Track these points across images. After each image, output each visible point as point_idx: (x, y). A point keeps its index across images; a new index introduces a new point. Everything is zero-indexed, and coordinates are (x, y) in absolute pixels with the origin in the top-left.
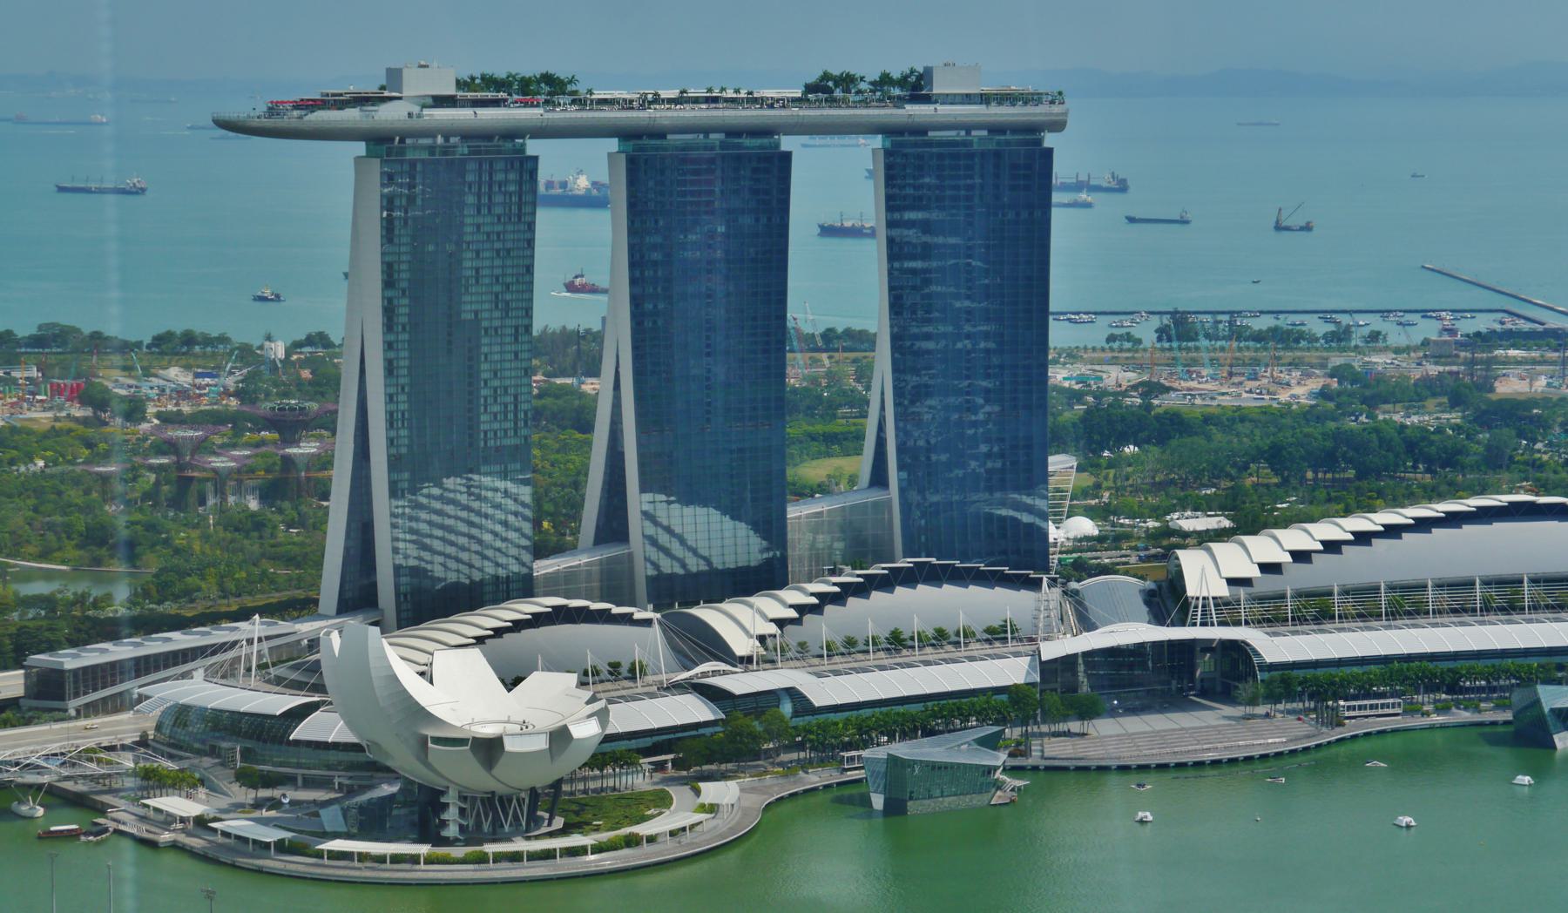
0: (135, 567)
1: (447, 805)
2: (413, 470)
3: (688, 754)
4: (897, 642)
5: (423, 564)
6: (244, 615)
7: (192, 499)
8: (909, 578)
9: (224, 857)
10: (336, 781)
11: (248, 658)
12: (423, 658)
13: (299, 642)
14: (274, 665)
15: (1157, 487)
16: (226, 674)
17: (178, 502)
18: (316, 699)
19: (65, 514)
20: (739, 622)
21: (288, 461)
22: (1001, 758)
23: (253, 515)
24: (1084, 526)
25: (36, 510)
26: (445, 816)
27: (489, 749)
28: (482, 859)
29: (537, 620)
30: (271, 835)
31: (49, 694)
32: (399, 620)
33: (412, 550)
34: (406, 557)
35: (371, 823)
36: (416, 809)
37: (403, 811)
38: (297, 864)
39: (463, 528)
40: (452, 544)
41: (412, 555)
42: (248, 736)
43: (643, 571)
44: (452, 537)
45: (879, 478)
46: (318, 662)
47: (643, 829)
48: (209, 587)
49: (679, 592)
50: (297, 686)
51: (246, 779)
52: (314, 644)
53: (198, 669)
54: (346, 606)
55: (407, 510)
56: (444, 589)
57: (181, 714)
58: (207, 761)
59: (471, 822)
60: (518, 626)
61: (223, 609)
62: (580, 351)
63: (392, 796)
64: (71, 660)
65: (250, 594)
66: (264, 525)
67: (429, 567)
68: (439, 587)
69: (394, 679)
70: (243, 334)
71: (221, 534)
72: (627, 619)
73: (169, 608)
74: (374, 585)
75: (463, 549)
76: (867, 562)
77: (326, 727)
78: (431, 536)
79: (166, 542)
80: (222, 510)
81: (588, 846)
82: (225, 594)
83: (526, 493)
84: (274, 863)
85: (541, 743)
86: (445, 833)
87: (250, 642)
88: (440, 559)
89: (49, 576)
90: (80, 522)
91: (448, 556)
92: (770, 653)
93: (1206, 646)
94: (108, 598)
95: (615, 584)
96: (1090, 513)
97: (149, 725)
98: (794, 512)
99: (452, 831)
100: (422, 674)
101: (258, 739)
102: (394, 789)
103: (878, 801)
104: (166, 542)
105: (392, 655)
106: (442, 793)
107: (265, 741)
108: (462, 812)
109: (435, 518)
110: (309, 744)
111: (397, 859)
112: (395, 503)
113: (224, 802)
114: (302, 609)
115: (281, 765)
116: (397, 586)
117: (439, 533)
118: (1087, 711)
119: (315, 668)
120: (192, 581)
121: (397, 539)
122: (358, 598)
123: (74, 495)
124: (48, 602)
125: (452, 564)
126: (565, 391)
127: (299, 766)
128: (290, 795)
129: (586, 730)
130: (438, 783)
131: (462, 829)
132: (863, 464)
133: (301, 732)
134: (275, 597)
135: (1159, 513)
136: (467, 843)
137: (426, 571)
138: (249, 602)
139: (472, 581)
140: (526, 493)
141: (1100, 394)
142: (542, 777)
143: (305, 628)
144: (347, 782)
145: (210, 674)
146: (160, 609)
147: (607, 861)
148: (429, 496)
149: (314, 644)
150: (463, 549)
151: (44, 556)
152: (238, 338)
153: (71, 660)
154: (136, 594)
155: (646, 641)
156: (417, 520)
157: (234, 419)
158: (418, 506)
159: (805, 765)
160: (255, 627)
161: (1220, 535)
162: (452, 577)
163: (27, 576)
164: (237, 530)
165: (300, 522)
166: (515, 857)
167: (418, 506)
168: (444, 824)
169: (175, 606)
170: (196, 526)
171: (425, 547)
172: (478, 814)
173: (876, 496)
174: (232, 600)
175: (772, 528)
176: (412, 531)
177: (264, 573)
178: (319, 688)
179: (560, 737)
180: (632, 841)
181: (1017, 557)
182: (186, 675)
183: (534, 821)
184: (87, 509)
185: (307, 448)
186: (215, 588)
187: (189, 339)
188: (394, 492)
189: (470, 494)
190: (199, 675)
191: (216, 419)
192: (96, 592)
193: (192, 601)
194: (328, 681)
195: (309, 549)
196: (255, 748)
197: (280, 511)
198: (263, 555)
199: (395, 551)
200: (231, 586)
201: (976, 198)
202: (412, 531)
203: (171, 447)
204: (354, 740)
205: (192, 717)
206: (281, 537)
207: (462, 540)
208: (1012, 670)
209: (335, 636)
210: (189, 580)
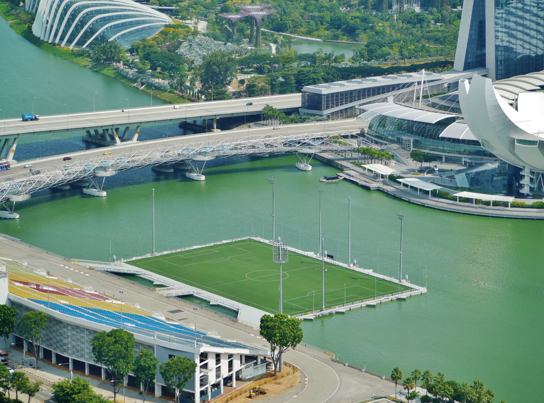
0: (355, 40)
1: (524, 176)
5: (511, 46)
7: (385, 5)
9: (398, 194)
10: (463, 160)
11: (418, 93)
12: (512, 96)
13: (444, 84)
14: (431, 96)
16: (407, 100)
18: (454, 116)
19: (320, 12)
23: (418, 15)
25: (305, 9)
26: (522, 182)
30: (430, 187)
32: (497, 75)
33: (505, 38)
34: (502, 41)
36: (506, 177)
37: (500, 178)
39: (534, 26)
40: (527, 35)
41: (505, 40)
42: (417, 134)
44: (528, 31)
46: (457, 96)
48: (394, 52)
51: (415, 156)
53: (390, 96)
54: (468, 66)
55: (504, 15)
56: (522, 58)
57: (383, 120)
58: (395, 146)
59: (535, 186)
61: (402, 65)
63: (493, 170)
65: (416, 57)
66: (423, 21)
67: (514, 47)
68: (519, 57)
69: (498, 107)
71: (401, 25)
73: (374, 63)
74: (484, 55)
75: (533, 37)
77: (459, 130)
78: (516, 30)
79: (372, 28)
82: (403, 57)
84: (431, 201)
86: (522, 191)
87: (419, 83)
88: (521, 43)
89: (310, 43)
90: (328, 16)
91: (525, 41)
94: (343, 56)
97: (365, 126)
99: (525, 190)
100: (511, 105)
101: (423, 136)
102: (495, 165)
104: (372, 28)
105: (497, 93)
106: (521, 170)
107: (426, 137)
108: (532, 180)
109: (519, 20)
110: (449, 139)
111: (496, 204)
112: (498, 11)
113: (404, 168)
114: (443, 67)
115: (434, 150)
116: (497, 57)
117: (520, 28)
119: (455, 99)
120: (386, 49)
121: (498, 31)
122: (475, 62)
124: (312, 58)
125: (527, 46)
127: (444, 151)
130: (519, 164)
131: (531, 189)
133: (446, 133)
134: (429, 60)
136: (534, 197)
137: (512, 49)
138: (415, 62)
139: (537, 56)
143: (447, 77)
144: (468, 161)
145: (397, 100)
146: (369, 63)
148: (516, 8)
150: (533, 37)
151: (309, 33)
154: (356, 56)
156: (509, 21)
158: (509, 13)
160: (422, 75)
162: (527, 52)
163: (300, 42)
164: (409, 22)
165: (442, 20)
167: (509, 13)
168: (521, 186)
169: (377, 62)
170: (387, 20)
171: (512, 36)
172: (540, 182)
174: (406, 60)
176: (506, 27)
177: (423, 46)
178: (457, 110)
182: (385, 100)
184: (331, 9)
186: (398, 54)
189: (538, 8)
190: (391, 99)
192: (337, 54)
193: (385, 60)
194: (462, 106)
195: (447, 34)
197: (431, 13)
198: (422, 37)
199: (497, 37)
200: (406, 53)
202: (506, 27)
204: (473, 138)
205: (388, 122)
206: (432, 27)
207: (533, 33)
209: (467, 82)
210: (384, 48)
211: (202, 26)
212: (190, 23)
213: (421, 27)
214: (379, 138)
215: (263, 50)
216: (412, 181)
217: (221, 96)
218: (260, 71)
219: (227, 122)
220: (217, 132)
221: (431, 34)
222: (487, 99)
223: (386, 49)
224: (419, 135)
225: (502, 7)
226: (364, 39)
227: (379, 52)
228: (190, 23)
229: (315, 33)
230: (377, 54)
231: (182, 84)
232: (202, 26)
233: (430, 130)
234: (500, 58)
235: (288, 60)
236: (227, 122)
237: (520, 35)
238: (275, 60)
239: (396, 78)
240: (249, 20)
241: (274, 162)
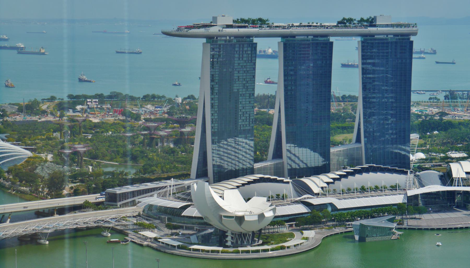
0: (137, 164)
1: (227, 236)
2: (218, 136)
3: (300, 222)
4: (363, 190)
5: (221, 164)
6: (169, 178)
7: (154, 143)
8: (367, 170)
10: (195, 228)
11: (170, 191)
12: (221, 192)
14: (177, 193)
15: (444, 144)
16: (164, 196)
17: (150, 145)
18: (189, 203)
19: (117, 148)
20: (315, 183)
21: (182, 133)
22: (394, 225)
23: (172, 149)
24: (421, 155)
25: (109, 146)
26: (227, 239)
27: (240, 219)
28: (238, 252)
29: (255, 181)
30: (176, 244)
31: (113, 200)
33: (218, 160)
34: (216, 162)
35: (205, 240)
37: (215, 237)
38: (184, 252)
39: (233, 153)
40: (230, 158)
41: (218, 162)
42: (169, 214)
43: (287, 167)
44: (230, 156)
45: (358, 140)
46: (190, 193)
47: (286, 244)
48: (158, 170)
49: (298, 173)
50: (184, 200)
51: (169, 227)
52: (189, 187)
53: (155, 194)
54: (199, 176)
56: (227, 171)
57: (150, 207)
58: (157, 221)
59: (235, 241)
60: (249, 183)
61: (163, 177)
62: (269, 101)
63: (211, 233)
64: (118, 191)
65: (170, 172)
67: (223, 165)
68: (226, 171)
70: (169, 95)
71: (162, 154)
72: (282, 182)
73: (147, 176)
74: (207, 170)
75: (233, 160)
76: (355, 165)
77: (192, 212)
78: (224, 156)
79: (146, 156)
80: (162, 147)
81: (269, 249)
82: (163, 172)
83: (252, 143)
84: (177, 252)
85: (256, 218)
86: (227, 244)
87: (170, 186)
88: (226, 163)
89: (112, 166)
91: (229, 162)
92: (324, 192)
93: (459, 192)
95: (278, 171)
96: (423, 151)
98: (333, 150)
99: (229, 244)
100: (221, 197)
101: (173, 215)
103: (357, 238)
104: (146, 156)
105: (212, 191)
106: (226, 232)
107: (174, 216)
108: (232, 238)
109: (225, 150)
111: (213, 251)
113: (162, 233)
116: (214, 170)
117: (226, 155)
118: (420, 212)
119: (189, 194)
120: (154, 168)
121: (214, 157)
122: (202, 174)
123: (120, 142)
124: (112, 173)
125: (230, 164)
126: (264, 113)
127: (184, 223)
128: (181, 232)
129: (269, 215)
130: (225, 229)
131: (232, 243)
132: (353, 136)
133: (185, 213)
134: (178, 173)
135: (444, 152)
136: (234, 247)
137: (222, 166)
138: (170, 174)
139: (236, 170)
140: (252, 143)
141: (426, 116)
142: (256, 228)
143: (186, 182)
144: (198, 228)
145: (159, 195)
146: (144, 176)
147: (275, 253)
148: (223, 144)
149: (189, 187)
150: (233, 160)
151: (111, 160)
152: (168, 96)
153: (118, 191)
154: (137, 172)
155: (288, 188)
156: (220, 151)
157: (167, 121)
158: (220, 147)
159: (335, 226)
160: (172, 182)
161: (463, 159)
162: (230, 168)
163: (106, 166)
164: (167, 153)
165: (185, 151)
166: (248, 252)
167: (220, 147)
168: (227, 241)
169: (149, 175)
170: (155, 152)
171: (222, 159)
172: (237, 239)
173: (358, 145)
174: (165, 174)
175: (326, 155)
176: (218, 154)
177: (175, 166)
178: (190, 200)
179: (261, 216)
180: (282, 248)
181: (401, 165)
182: (152, 196)
183: (253, 241)
185: (187, 129)
186: (160, 170)
187: (154, 97)
188: (213, 142)
189: (235, 143)
191: (162, 120)
192: (126, 171)
193: (154, 174)
194: (193, 198)
195: (188, 159)
196: (171, 218)
197: (179, 148)
198: (174, 161)
199: (213, 160)
200: (165, 170)
201: (389, 56)
202: (218, 154)
203: (148, 128)
205: (153, 208)
206: (180, 155)
207: (233, 157)
208: (398, 199)
209: (195, 186)
210: (153, 168)
211: (50, 157)
212: (43, 156)
213: (174, 155)
214: (148, 217)
215: (85, 170)
216: (166, 240)
217: (60, 196)
218: (82, 181)
219: (61, 211)
220: (56, 216)
221: (179, 159)
222: (206, 193)
223: (154, 168)
224: (170, 215)
225: (216, 144)
226: (142, 163)
227: (150, 170)
228: (43, 156)
229: (115, 160)
230: (149, 171)
231: (37, 189)
232: (50, 157)
233: (176, 212)
234: (215, 171)
235: (99, 175)
236: (61, 211)
237: (226, 158)
238: (91, 175)
239: (158, 184)
240: (76, 153)
241: (89, 232)
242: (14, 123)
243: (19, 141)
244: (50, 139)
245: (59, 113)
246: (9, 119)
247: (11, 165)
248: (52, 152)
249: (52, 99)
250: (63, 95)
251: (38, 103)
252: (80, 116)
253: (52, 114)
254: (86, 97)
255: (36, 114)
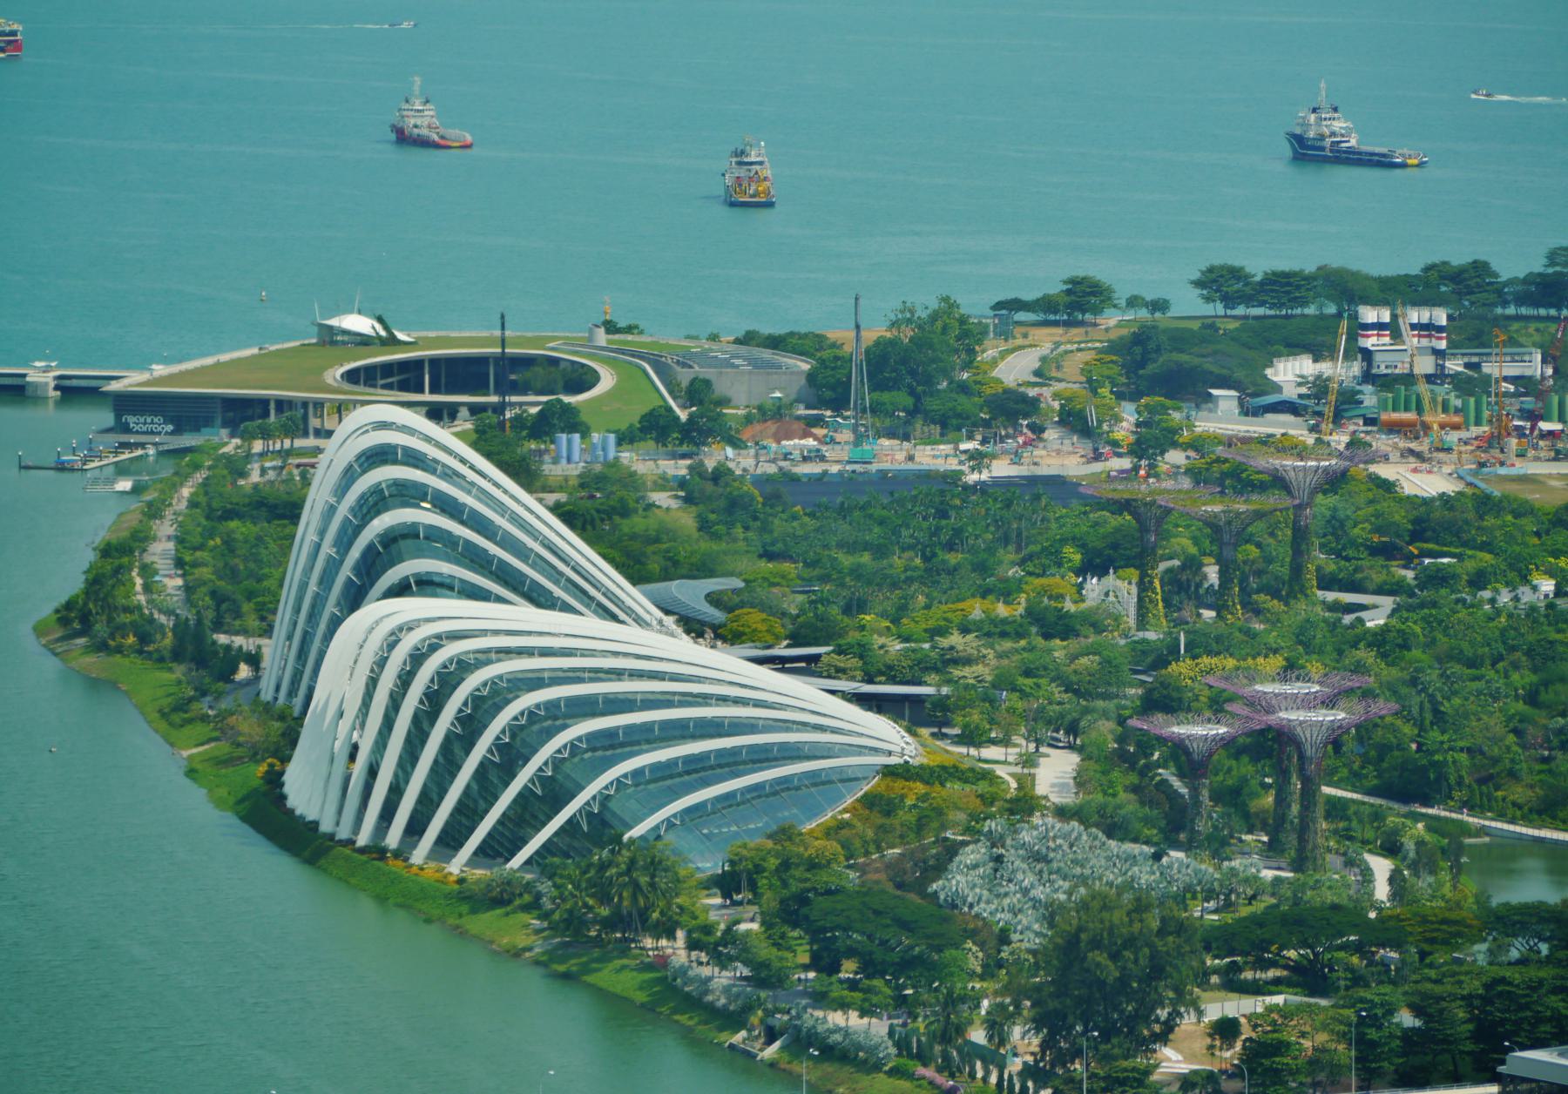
25: (1532, 698)
211: (1056, 772)
215: (1331, 880)
218: (1310, 978)
231: (950, 1032)
232: (1056, 772)
235: (1445, 931)
238: (1388, 931)
240: (1271, 745)
242: (780, 489)
243: (807, 644)
244: (1057, 626)
245: (1129, 415)
246: (742, 462)
247: (752, 833)
248: (1071, 730)
249: (1079, 300)
250: (1160, 277)
251: (969, 336)
252: (1302, 449)
253: (1074, 421)
254: (1348, 289)
255: (949, 424)
